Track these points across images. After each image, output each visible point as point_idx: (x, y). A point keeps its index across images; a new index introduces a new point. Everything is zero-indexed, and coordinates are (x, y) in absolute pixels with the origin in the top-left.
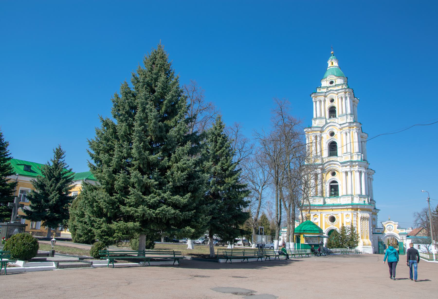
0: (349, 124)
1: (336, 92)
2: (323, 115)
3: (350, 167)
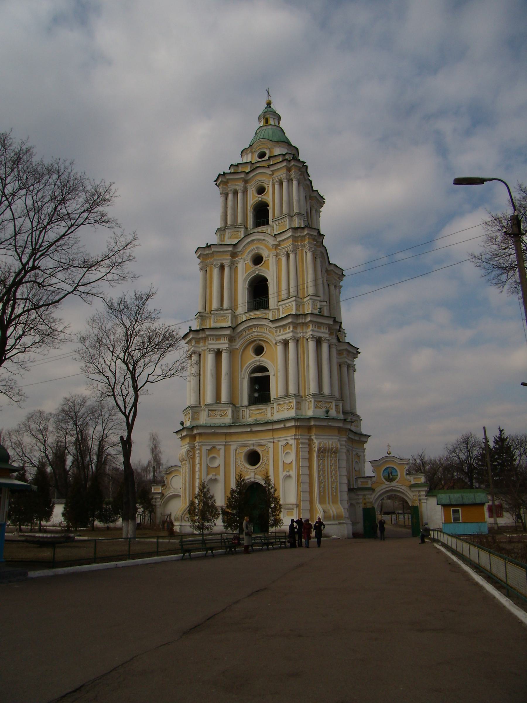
0: (292, 232)
1: (268, 171)
2: (239, 220)
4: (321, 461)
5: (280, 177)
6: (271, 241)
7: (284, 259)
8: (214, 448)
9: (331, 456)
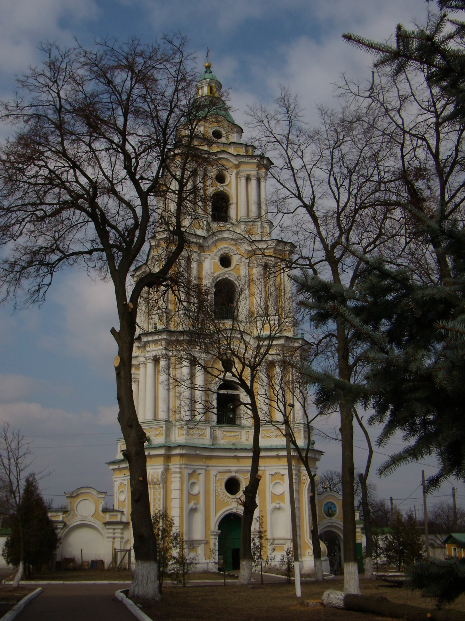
5: (249, 172)
8: (194, 472)
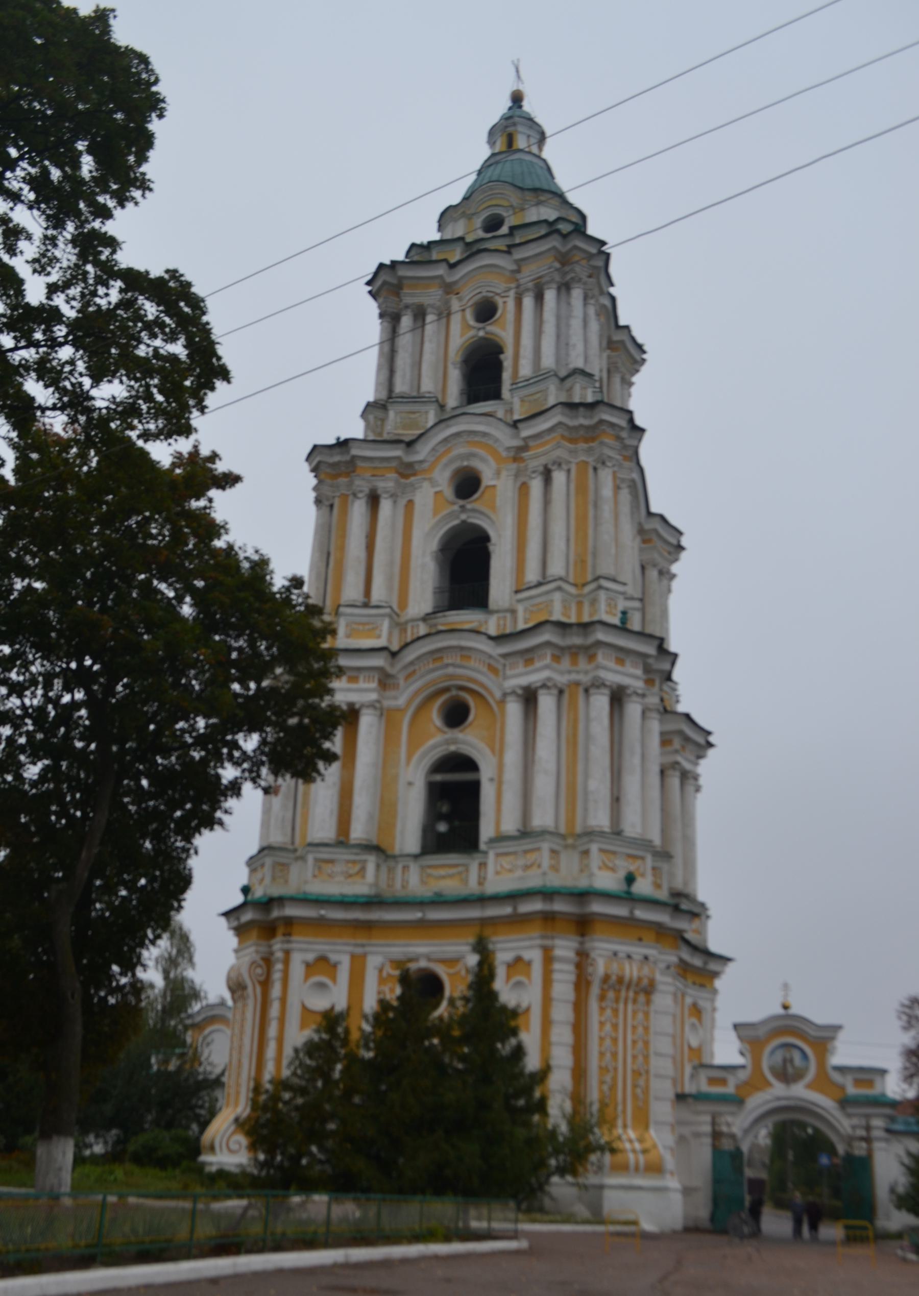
3: (556, 658)
4: (609, 1012)
6: (505, 438)
7: (536, 486)
8: (322, 959)
9: (635, 1001)
